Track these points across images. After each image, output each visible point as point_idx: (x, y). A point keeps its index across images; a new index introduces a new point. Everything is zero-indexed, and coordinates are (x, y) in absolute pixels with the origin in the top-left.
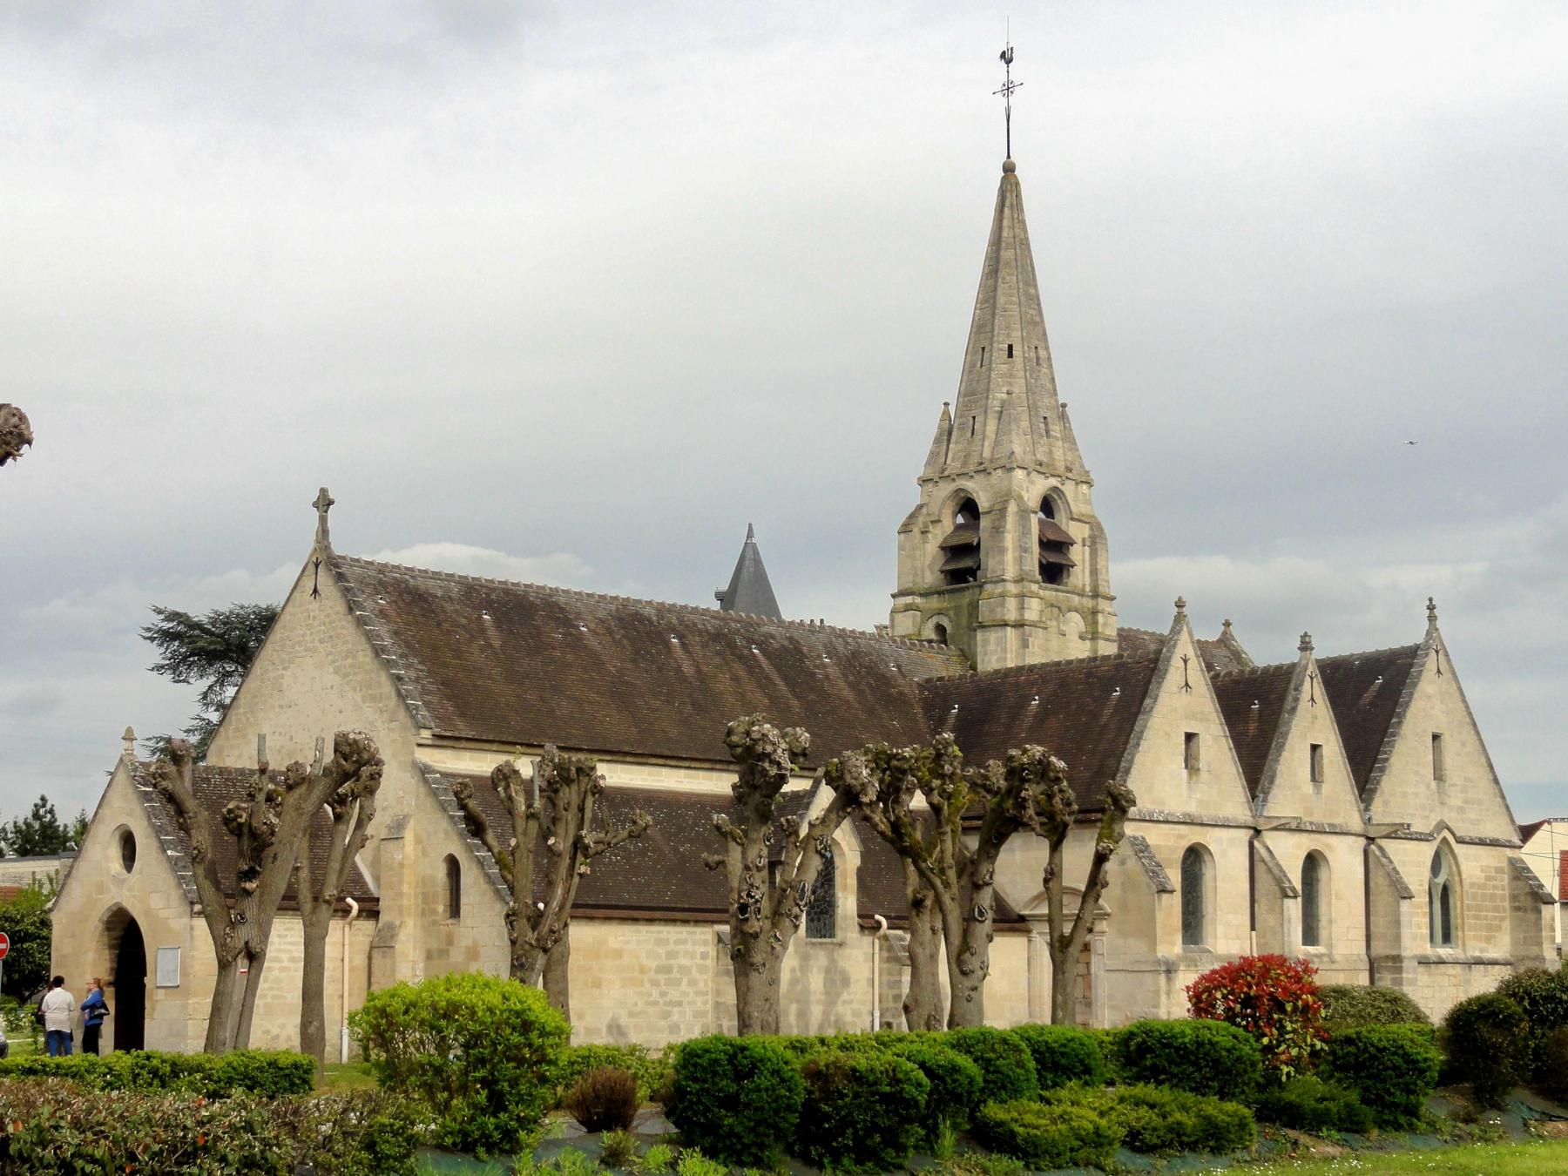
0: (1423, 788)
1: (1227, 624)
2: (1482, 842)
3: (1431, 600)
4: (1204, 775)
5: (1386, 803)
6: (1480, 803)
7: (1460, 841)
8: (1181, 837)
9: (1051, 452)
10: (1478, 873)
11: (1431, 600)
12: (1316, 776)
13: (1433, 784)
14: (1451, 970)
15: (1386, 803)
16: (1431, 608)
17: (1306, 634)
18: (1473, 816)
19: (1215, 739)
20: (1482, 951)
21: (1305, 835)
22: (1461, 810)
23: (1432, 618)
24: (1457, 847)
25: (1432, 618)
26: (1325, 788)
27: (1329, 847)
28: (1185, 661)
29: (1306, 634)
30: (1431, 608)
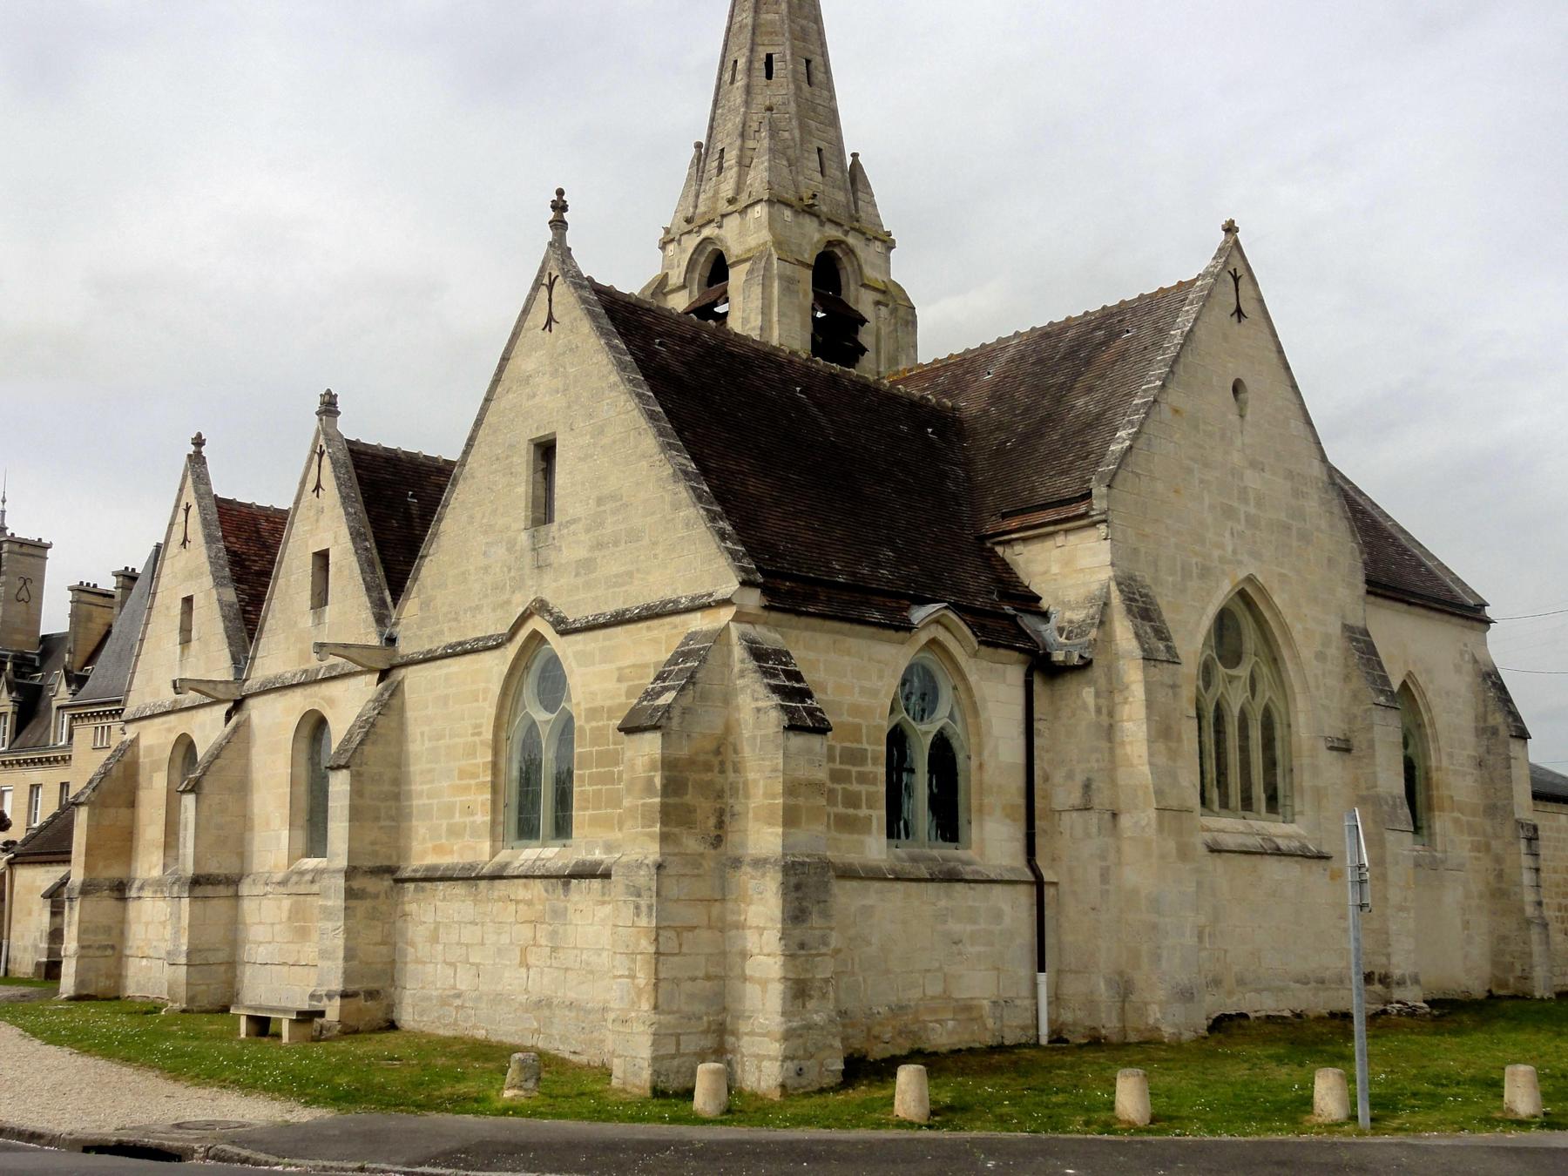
0: (500, 552)
1: (1230, 228)
2: (620, 620)
3: (560, 193)
4: (194, 644)
5: (425, 605)
6: (633, 536)
7: (565, 628)
8: (169, 730)
9: (716, 192)
10: (611, 685)
11: (560, 193)
12: (320, 598)
13: (524, 538)
14: (519, 890)
15: (425, 605)
16: (560, 206)
17: (329, 392)
18: (615, 568)
19: (208, 595)
20: (609, 848)
21: (299, 692)
22: (587, 565)
23: (559, 225)
24: (554, 641)
25: (559, 225)
26: (330, 611)
27: (331, 702)
28: (187, 510)
29: (329, 392)
30: (560, 206)
